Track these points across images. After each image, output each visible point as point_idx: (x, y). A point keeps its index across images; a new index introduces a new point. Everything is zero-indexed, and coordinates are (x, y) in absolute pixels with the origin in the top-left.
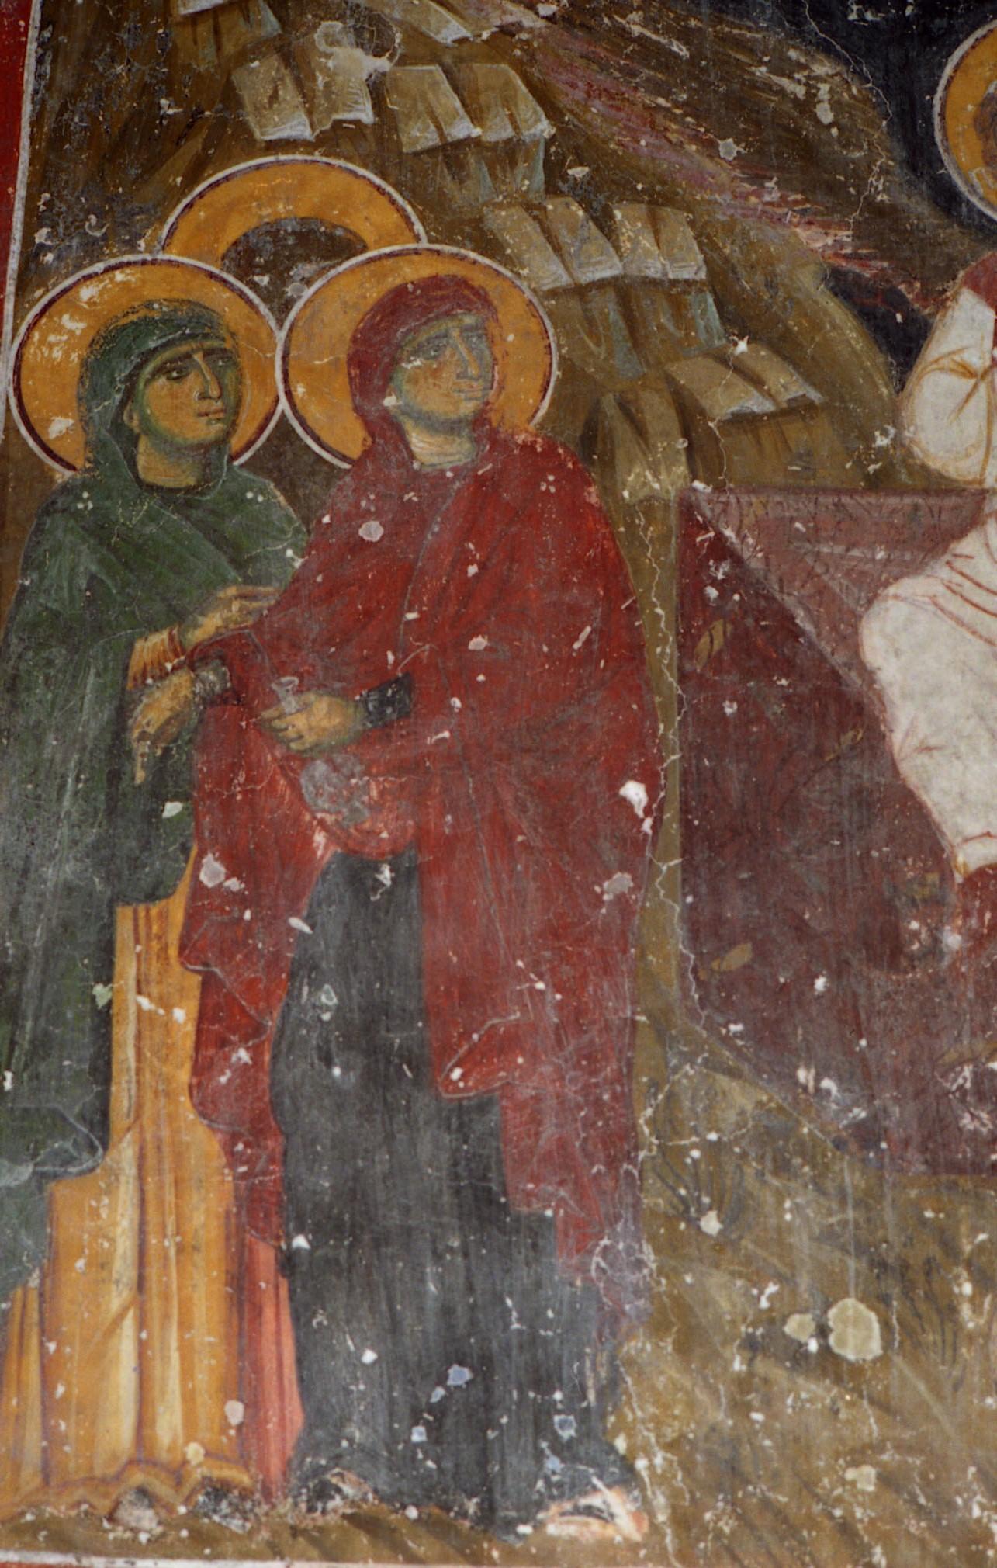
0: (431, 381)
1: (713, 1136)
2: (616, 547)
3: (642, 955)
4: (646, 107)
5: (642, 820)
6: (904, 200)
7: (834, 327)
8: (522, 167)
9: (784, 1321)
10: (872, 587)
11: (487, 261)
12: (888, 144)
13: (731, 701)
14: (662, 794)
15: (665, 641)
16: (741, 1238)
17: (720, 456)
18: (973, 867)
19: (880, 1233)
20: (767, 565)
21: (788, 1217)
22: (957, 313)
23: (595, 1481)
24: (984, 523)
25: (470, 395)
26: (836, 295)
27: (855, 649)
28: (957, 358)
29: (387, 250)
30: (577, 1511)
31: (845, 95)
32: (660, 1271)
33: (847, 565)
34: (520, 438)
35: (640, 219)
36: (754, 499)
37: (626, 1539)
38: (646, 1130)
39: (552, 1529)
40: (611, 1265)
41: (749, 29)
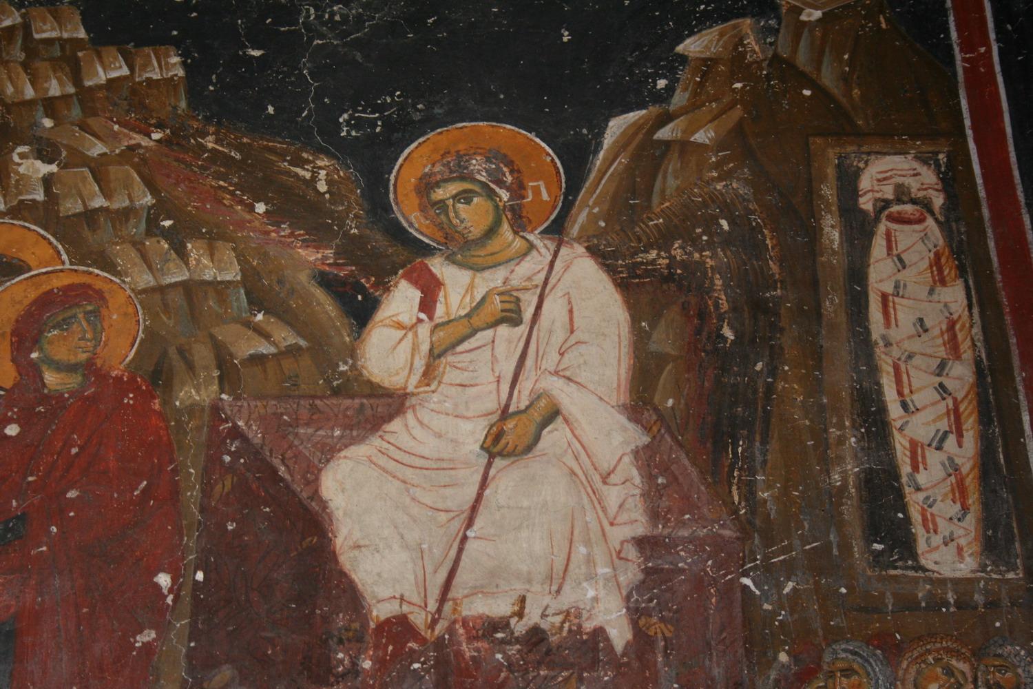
0: (62, 342)
2: (168, 435)
3: (157, 680)
4: (212, 187)
5: (167, 596)
6: (368, 232)
7: (319, 304)
8: (133, 221)
10: (329, 452)
11: (106, 275)
12: (360, 201)
13: (232, 522)
14: (181, 580)
17: (239, 380)
18: (382, 618)
20: (264, 441)
22: (396, 294)
24: (405, 413)
25: (85, 349)
26: (321, 286)
27: (316, 492)
28: (394, 319)
29: (44, 270)
31: (336, 176)
34: (114, 374)
35: (202, 248)
36: (259, 404)
41: (280, 143)
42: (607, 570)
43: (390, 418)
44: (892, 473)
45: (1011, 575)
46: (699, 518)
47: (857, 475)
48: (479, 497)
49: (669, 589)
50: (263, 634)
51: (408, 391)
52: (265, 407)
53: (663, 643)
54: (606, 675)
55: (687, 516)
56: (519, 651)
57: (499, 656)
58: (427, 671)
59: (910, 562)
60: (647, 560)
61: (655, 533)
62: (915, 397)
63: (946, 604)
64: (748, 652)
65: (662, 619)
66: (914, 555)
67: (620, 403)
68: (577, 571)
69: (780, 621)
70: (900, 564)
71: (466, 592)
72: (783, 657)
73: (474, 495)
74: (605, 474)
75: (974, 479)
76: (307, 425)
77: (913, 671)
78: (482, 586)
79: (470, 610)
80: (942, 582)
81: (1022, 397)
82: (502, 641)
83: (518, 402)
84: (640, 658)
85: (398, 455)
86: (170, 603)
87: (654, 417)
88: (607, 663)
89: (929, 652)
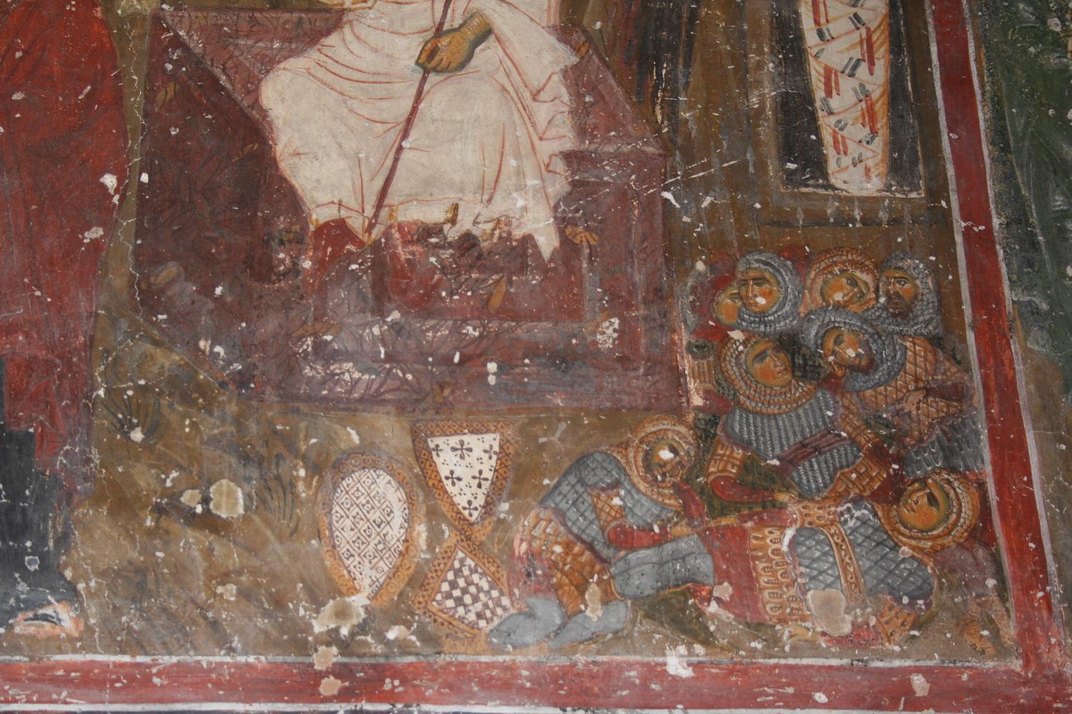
1: (142, 382)
3: (106, 274)
9: (181, 493)
10: (269, 63)
15: (136, 94)
16: (156, 444)
18: (322, 221)
19: (247, 439)
21: (187, 430)
23: (49, 597)
24: (342, 27)
27: (257, 100)
30: (36, 618)
32: (102, 465)
33: (255, 50)
36: (199, 14)
37: (68, 635)
38: (99, 380)
39: (17, 630)
40: (70, 462)
42: (537, 182)
43: (328, 32)
44: (807, 97)
45: (913, 195)
46: (624, 135)
47: (774, 98)
48: (414, 110)
49: (595, 201)
50: (207, 234)
51: (345, 7)
52: (206, 18)
53: (588, 251)
54: (534, 279)
55: (613, 133)
56: (452, 255)
57: (433, 260)
58: (365, 272)
59: (821, 181)
60: (574, 173)
61: (583, 147)
62: (830, 26)
63: (853, 220)
64: (668, 261)
65: (587, 229)
66: (825, 175)
67: (550, 24)
68: (507, 181)
69: (699, 233)
70: (811, 182)
71: (401, 199)
72: (700, 266)
73: (409, 109)
74: (535, 92)
75: (883, 104)
76: (247, 36)
77: (820, 281)
78: (417, 194)
79: (405, 215)
80: (850, 200)
81: (931, 29)
82: (436, 246)
83: (452, 20)
84: (567, 262)
85: (335, 68)
86: (117, 203)
87: (583, 39)
88: (535, 268)
89: (835, 263)
